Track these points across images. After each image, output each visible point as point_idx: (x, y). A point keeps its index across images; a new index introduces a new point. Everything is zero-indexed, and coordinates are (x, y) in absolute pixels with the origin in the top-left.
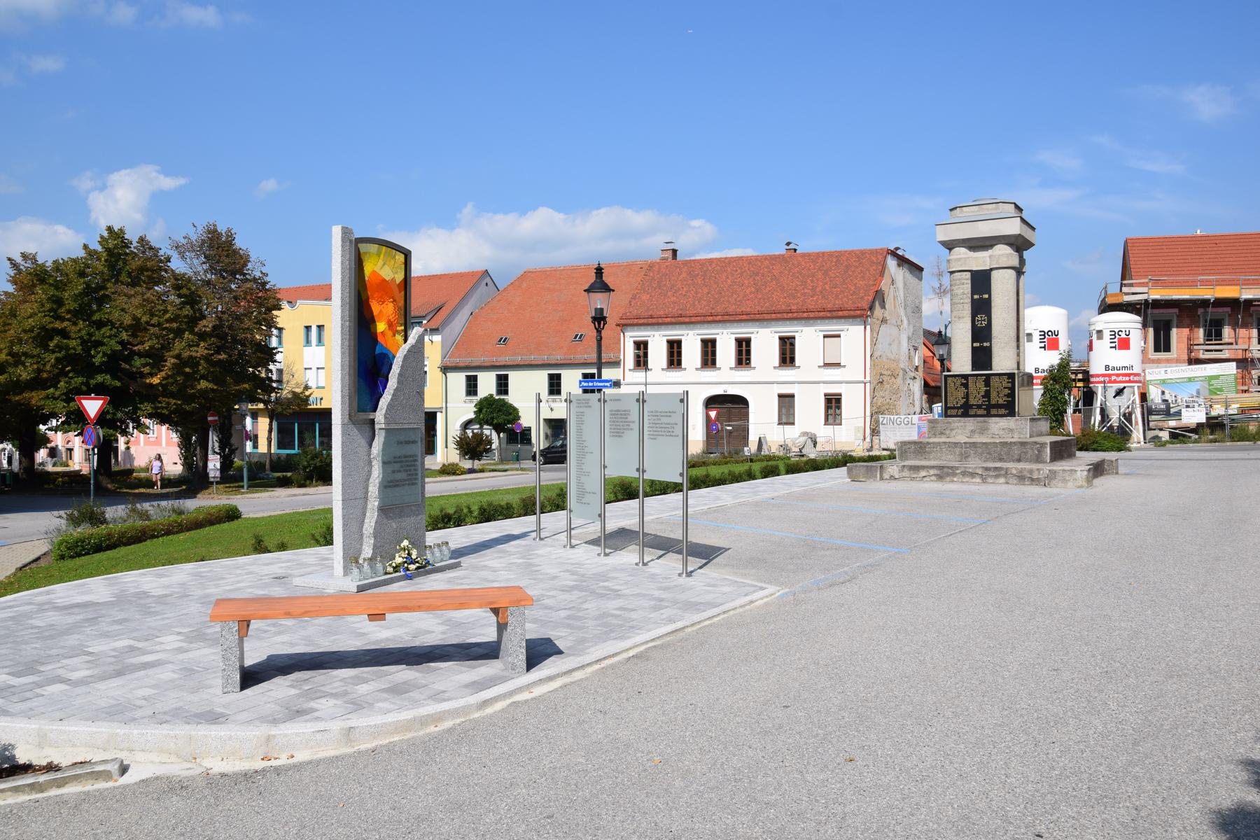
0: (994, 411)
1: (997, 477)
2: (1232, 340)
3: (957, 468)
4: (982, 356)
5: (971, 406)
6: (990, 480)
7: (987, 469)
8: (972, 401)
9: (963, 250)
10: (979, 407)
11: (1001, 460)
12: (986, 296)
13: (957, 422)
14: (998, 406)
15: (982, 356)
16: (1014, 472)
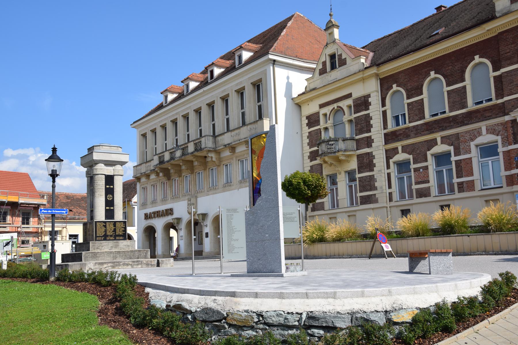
0: (117, 238)
1: (138, 265)
2: (11, 222)
3: (121, 262)
4: (110, 213)
5: (108, 236)
6: (135, 267)
7: (133, 262)
8: (108, 233)
9: (103, 165)
10: (111, 236)
11: (131, 258)
12: (112, 187)
13: (104, 243)
15: (110, 213)
16: (145, 262)
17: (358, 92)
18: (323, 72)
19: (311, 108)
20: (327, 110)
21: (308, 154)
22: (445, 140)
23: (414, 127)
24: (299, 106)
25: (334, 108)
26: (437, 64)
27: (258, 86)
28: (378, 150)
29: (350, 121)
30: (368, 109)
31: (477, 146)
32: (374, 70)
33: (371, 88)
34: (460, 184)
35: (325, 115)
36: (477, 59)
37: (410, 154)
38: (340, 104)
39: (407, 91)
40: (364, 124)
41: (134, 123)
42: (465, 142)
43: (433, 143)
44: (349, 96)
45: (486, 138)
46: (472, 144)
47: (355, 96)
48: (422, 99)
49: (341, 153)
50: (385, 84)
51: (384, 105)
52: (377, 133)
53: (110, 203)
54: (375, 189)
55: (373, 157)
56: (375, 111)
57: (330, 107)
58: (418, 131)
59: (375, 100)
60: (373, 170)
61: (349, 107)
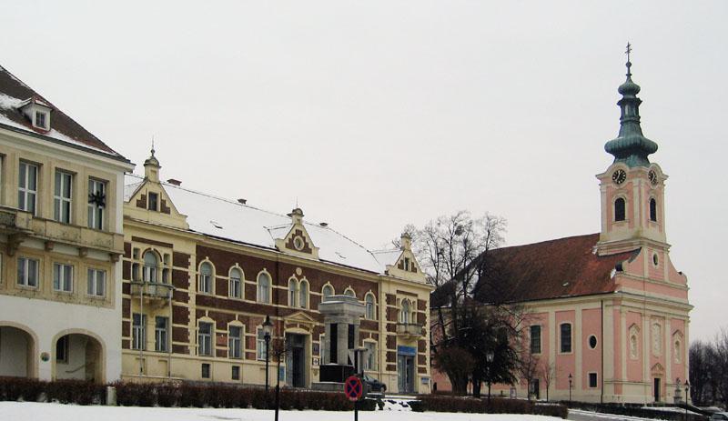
22: (241, 319)
25: (150, 249)
28: (191, 306)
34: (247, 353)
36: (265, 271)
37: (214, 319)
38: (159, 249)
40: (181, 280)
43: (233, 318)
51: (197, 270)
54: (188, 341)
57: (146, 246)
58: (223, 304)
59: (192, 260)
60: (187, 324)
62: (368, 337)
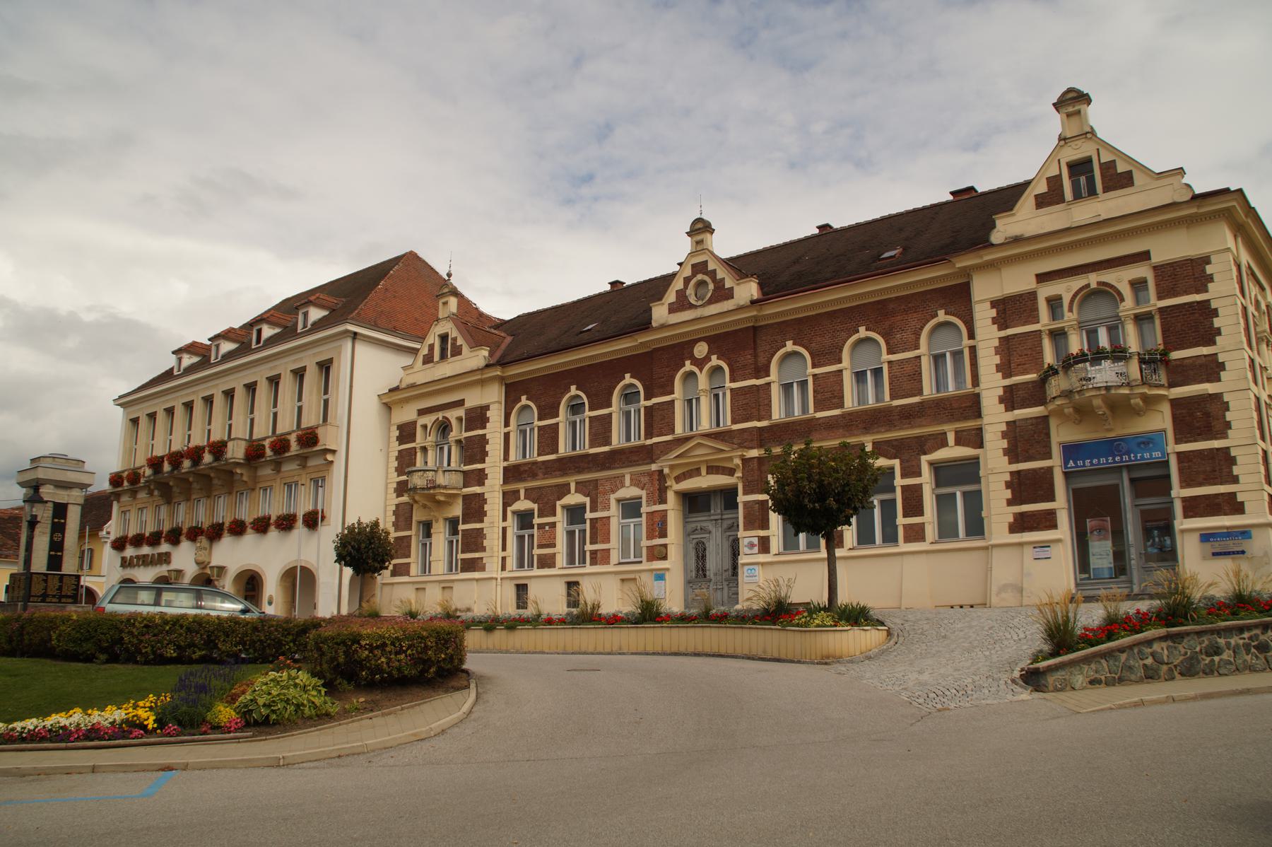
4: (55, 561)
10: (54, 596)
14: (67, 597)
15: (55, 561)
17: (473, 399)
18: (428, 359)
19: (407, 414)
20: (428, 420)
21: (395, 485)
22: (582, 488)
23: (544, 462)
24: (388, 407)
26: (580, 375)
27: (325, 367)
28: (493, 489)
29: (459, 442)
30: (484, 427)
31: (618, 501)
32: (498, 372)
33: (492, 396)
34: (594, 553)
35: (425, 427)
39: (539, 408)
40: (475, 450)
41: (121, 397)
42: (605, 493)
43: (563, 490)
44: (461, 403)
45: (629, 491)
46: (613, 497)
47: (468, 404)
48: (557, 424)
49: (437, 491)
50: (513, 391)
51: (507, 424)
52: (494, 465)
53: (56, 547)
54: (484, 549)
55: (485, 501)
56: (494, 431)
59: (495, 415)
60: (482, 521)
61: (460, 419)
62: (944, 444)
